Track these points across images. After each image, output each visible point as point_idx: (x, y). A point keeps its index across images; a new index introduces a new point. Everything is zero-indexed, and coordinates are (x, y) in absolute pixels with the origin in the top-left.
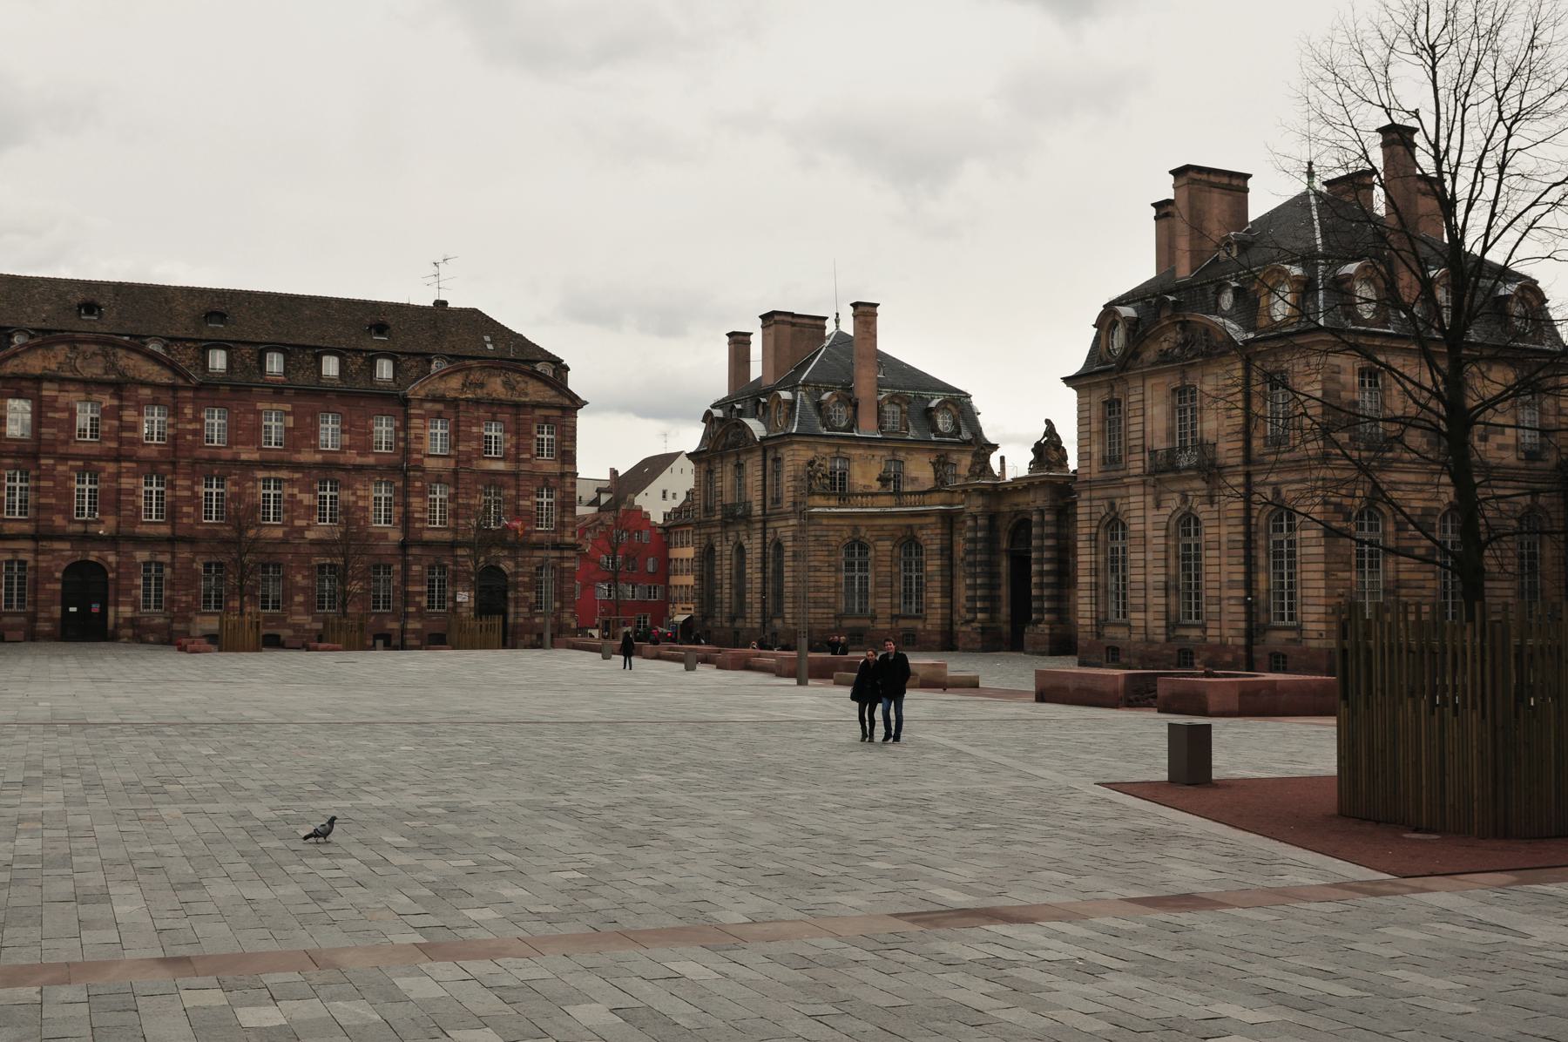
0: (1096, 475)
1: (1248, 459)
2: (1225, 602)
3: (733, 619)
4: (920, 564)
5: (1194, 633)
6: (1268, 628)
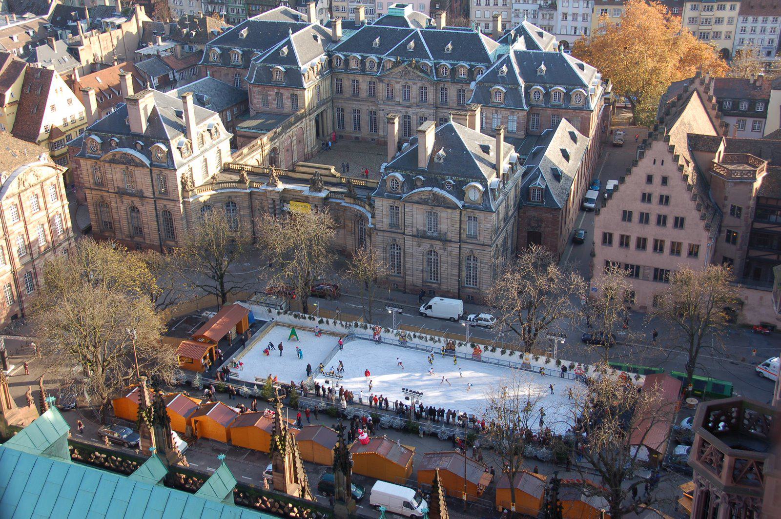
0: (385, 229)
1: (460, 241)
2: (449, 280)
3: (132, 237)
4: (235, 210)
5: (434, 286)
6: (465, 287)
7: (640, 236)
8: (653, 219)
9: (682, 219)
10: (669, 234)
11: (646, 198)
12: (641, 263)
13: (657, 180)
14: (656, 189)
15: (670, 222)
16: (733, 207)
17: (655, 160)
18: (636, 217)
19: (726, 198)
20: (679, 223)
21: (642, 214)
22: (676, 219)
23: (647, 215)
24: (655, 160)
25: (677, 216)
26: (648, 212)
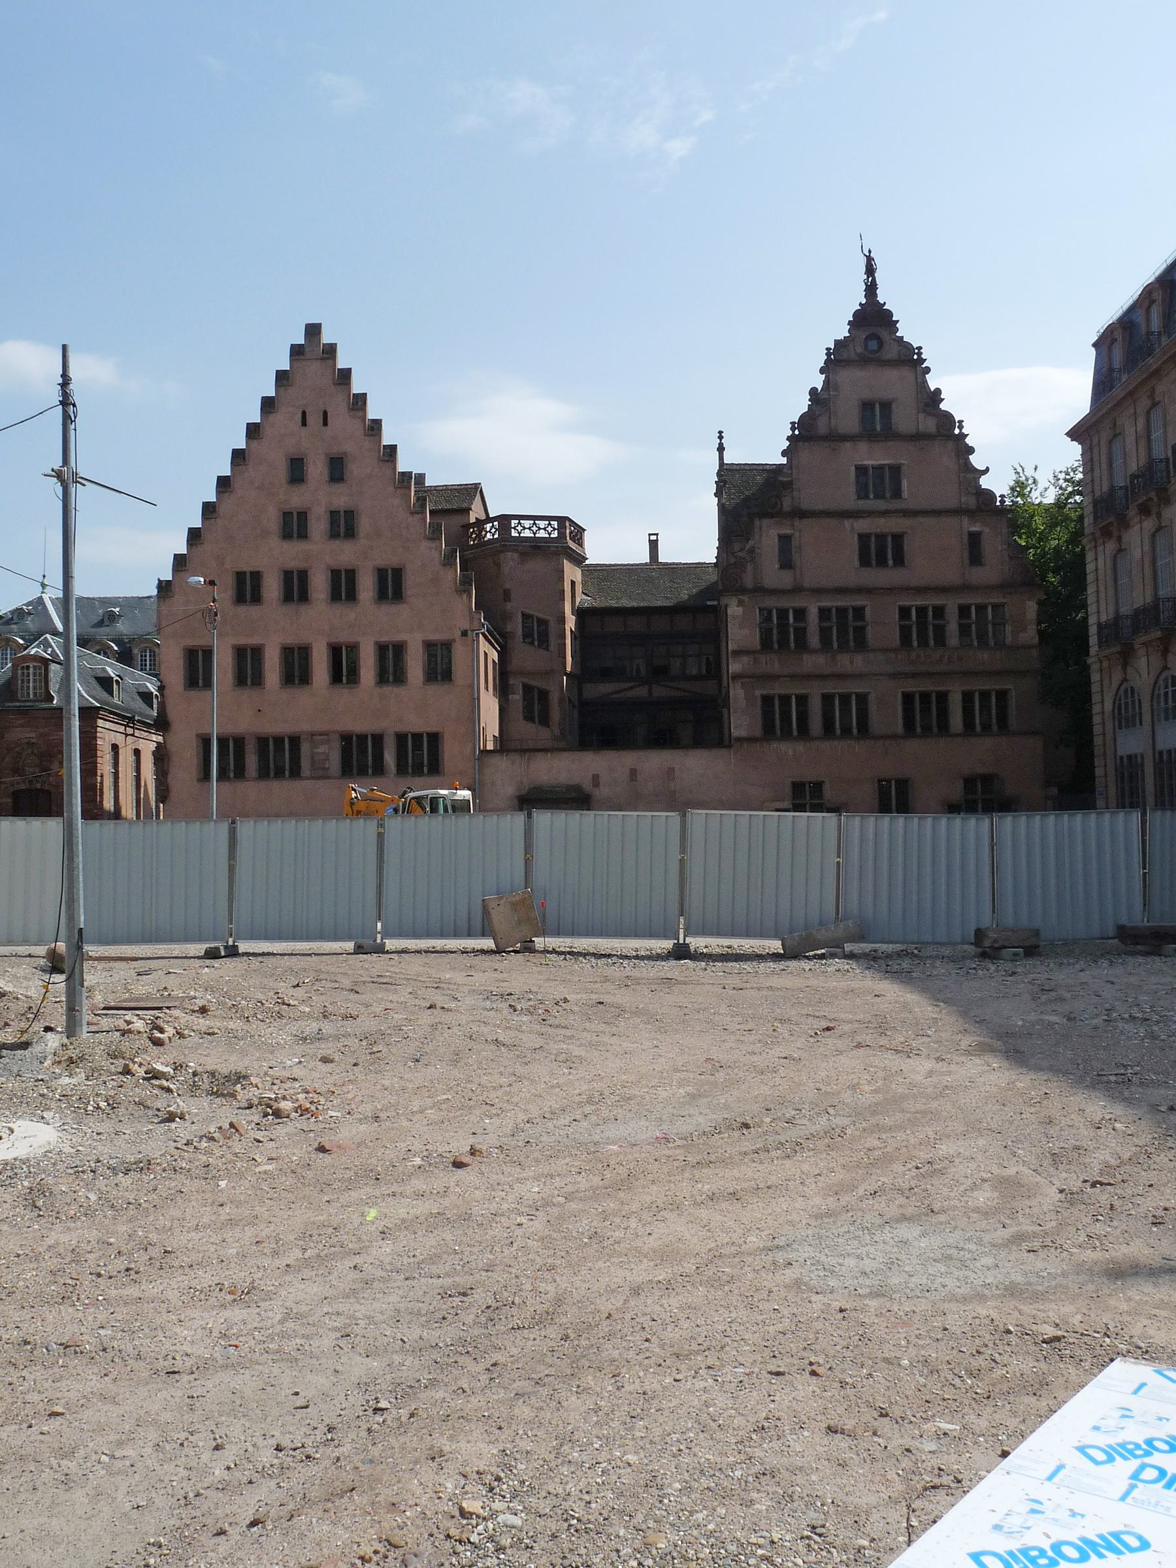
7: (291, 640)
8: (319, 584)
9: (398, 573)
10: (368, 623)
11: (294, 526)
12: (305, 727)
13: (317, 469)
14: (318, 497)
15: (366, 586)
16: (526, 617)
17: (304, 413)
18: (272, 587)
19: (507, 596)
20: (391, 585)
21: (288, 575)
22: (381, 573)
23: (303, 575)
24: (304, 413)
25: (381, 562)
26: (302, 565)
